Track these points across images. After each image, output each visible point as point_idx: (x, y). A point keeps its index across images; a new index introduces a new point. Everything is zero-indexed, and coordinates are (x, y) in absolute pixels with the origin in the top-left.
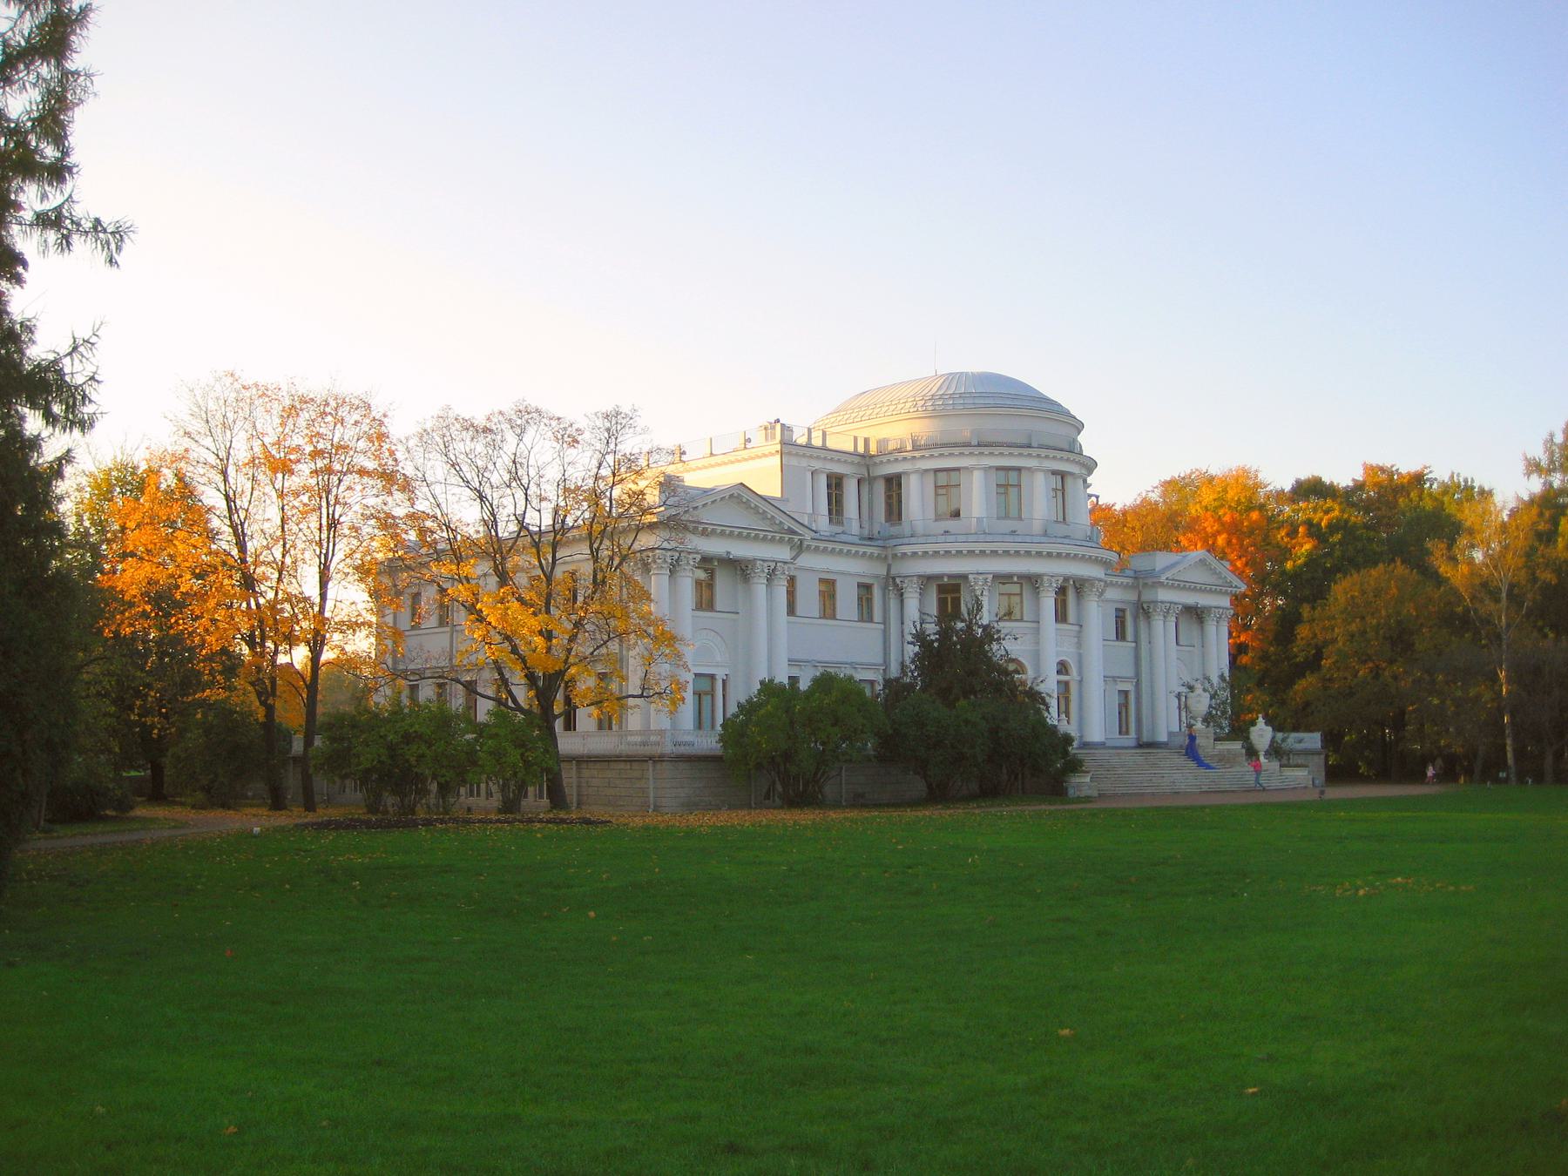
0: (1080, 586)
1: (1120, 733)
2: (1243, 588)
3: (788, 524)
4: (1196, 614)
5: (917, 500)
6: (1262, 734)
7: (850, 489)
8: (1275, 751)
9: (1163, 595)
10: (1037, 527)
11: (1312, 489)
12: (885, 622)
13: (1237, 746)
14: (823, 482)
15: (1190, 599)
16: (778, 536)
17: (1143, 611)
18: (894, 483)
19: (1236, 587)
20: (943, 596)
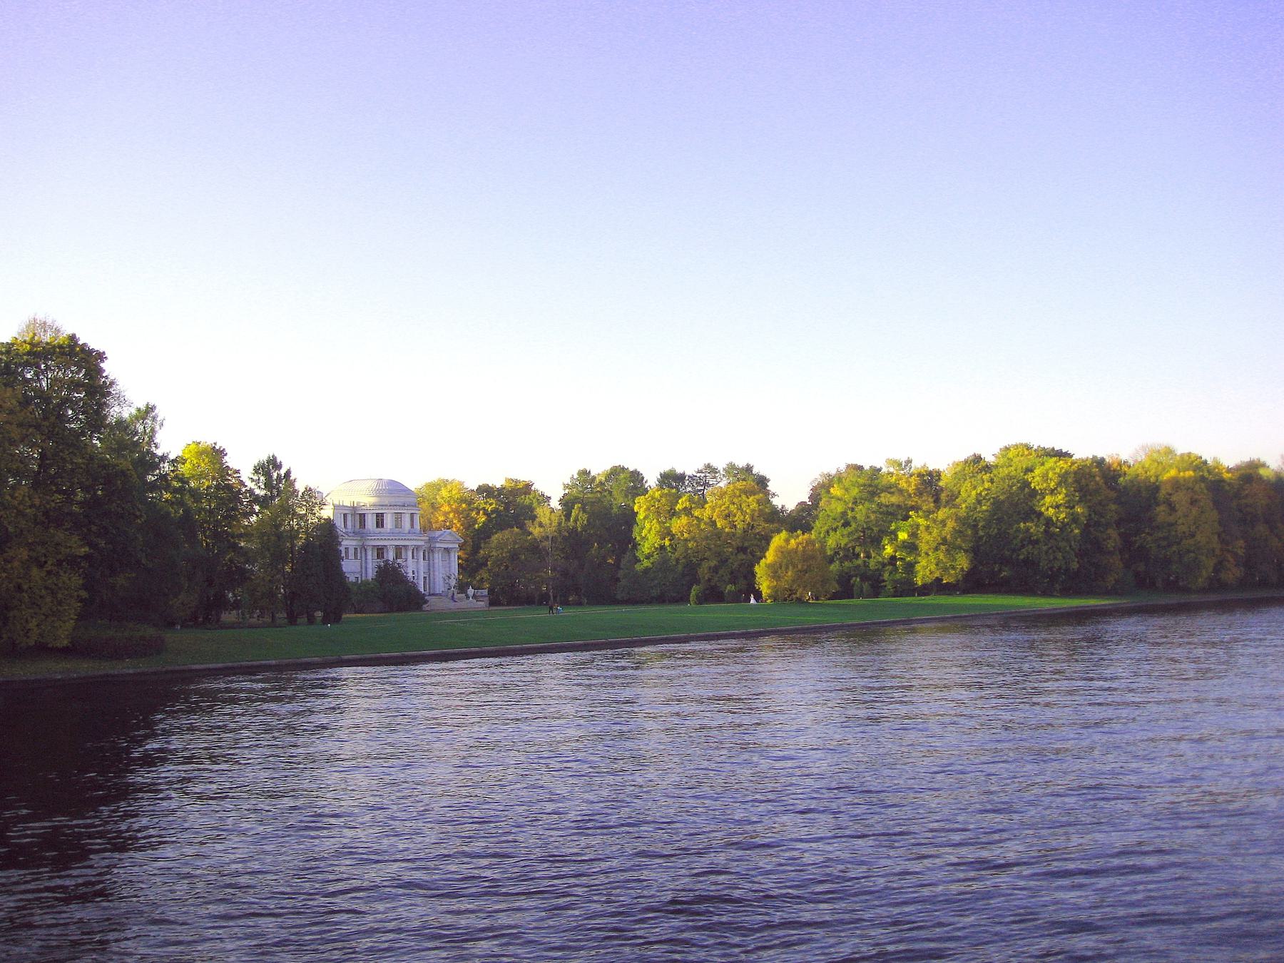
0: (418, 548)
4: (447, 550)
5: (371, 522)
6: (471, 591)
7: (349, 518)
8: (474, 596)
9: (438, 545)
10: (407, 531)
11: (486, 491)
12: (361, 559)
13: (464, 595)
15: (446, 546)
17: (431, 550)
18: (362, 516)
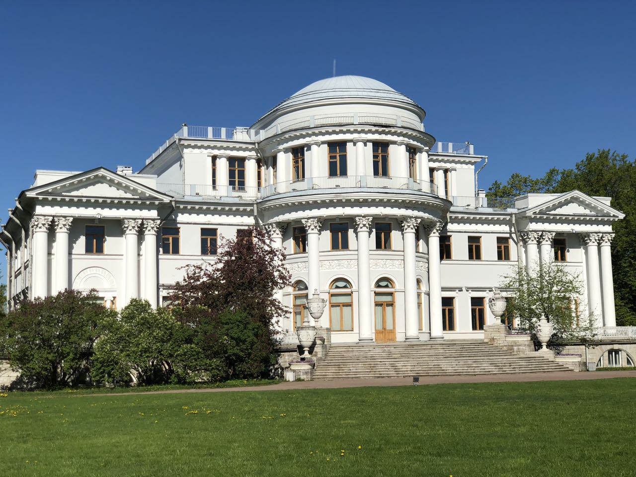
1: (474, 328)
2: (622, 216)
3: (148, 193)
9: (533, 226)
14: (223, 166)
16: (140, 202)
17: (523, 238)
19: (614, 216)
20: (204, 237)
